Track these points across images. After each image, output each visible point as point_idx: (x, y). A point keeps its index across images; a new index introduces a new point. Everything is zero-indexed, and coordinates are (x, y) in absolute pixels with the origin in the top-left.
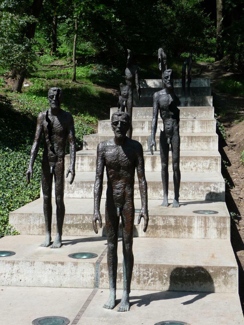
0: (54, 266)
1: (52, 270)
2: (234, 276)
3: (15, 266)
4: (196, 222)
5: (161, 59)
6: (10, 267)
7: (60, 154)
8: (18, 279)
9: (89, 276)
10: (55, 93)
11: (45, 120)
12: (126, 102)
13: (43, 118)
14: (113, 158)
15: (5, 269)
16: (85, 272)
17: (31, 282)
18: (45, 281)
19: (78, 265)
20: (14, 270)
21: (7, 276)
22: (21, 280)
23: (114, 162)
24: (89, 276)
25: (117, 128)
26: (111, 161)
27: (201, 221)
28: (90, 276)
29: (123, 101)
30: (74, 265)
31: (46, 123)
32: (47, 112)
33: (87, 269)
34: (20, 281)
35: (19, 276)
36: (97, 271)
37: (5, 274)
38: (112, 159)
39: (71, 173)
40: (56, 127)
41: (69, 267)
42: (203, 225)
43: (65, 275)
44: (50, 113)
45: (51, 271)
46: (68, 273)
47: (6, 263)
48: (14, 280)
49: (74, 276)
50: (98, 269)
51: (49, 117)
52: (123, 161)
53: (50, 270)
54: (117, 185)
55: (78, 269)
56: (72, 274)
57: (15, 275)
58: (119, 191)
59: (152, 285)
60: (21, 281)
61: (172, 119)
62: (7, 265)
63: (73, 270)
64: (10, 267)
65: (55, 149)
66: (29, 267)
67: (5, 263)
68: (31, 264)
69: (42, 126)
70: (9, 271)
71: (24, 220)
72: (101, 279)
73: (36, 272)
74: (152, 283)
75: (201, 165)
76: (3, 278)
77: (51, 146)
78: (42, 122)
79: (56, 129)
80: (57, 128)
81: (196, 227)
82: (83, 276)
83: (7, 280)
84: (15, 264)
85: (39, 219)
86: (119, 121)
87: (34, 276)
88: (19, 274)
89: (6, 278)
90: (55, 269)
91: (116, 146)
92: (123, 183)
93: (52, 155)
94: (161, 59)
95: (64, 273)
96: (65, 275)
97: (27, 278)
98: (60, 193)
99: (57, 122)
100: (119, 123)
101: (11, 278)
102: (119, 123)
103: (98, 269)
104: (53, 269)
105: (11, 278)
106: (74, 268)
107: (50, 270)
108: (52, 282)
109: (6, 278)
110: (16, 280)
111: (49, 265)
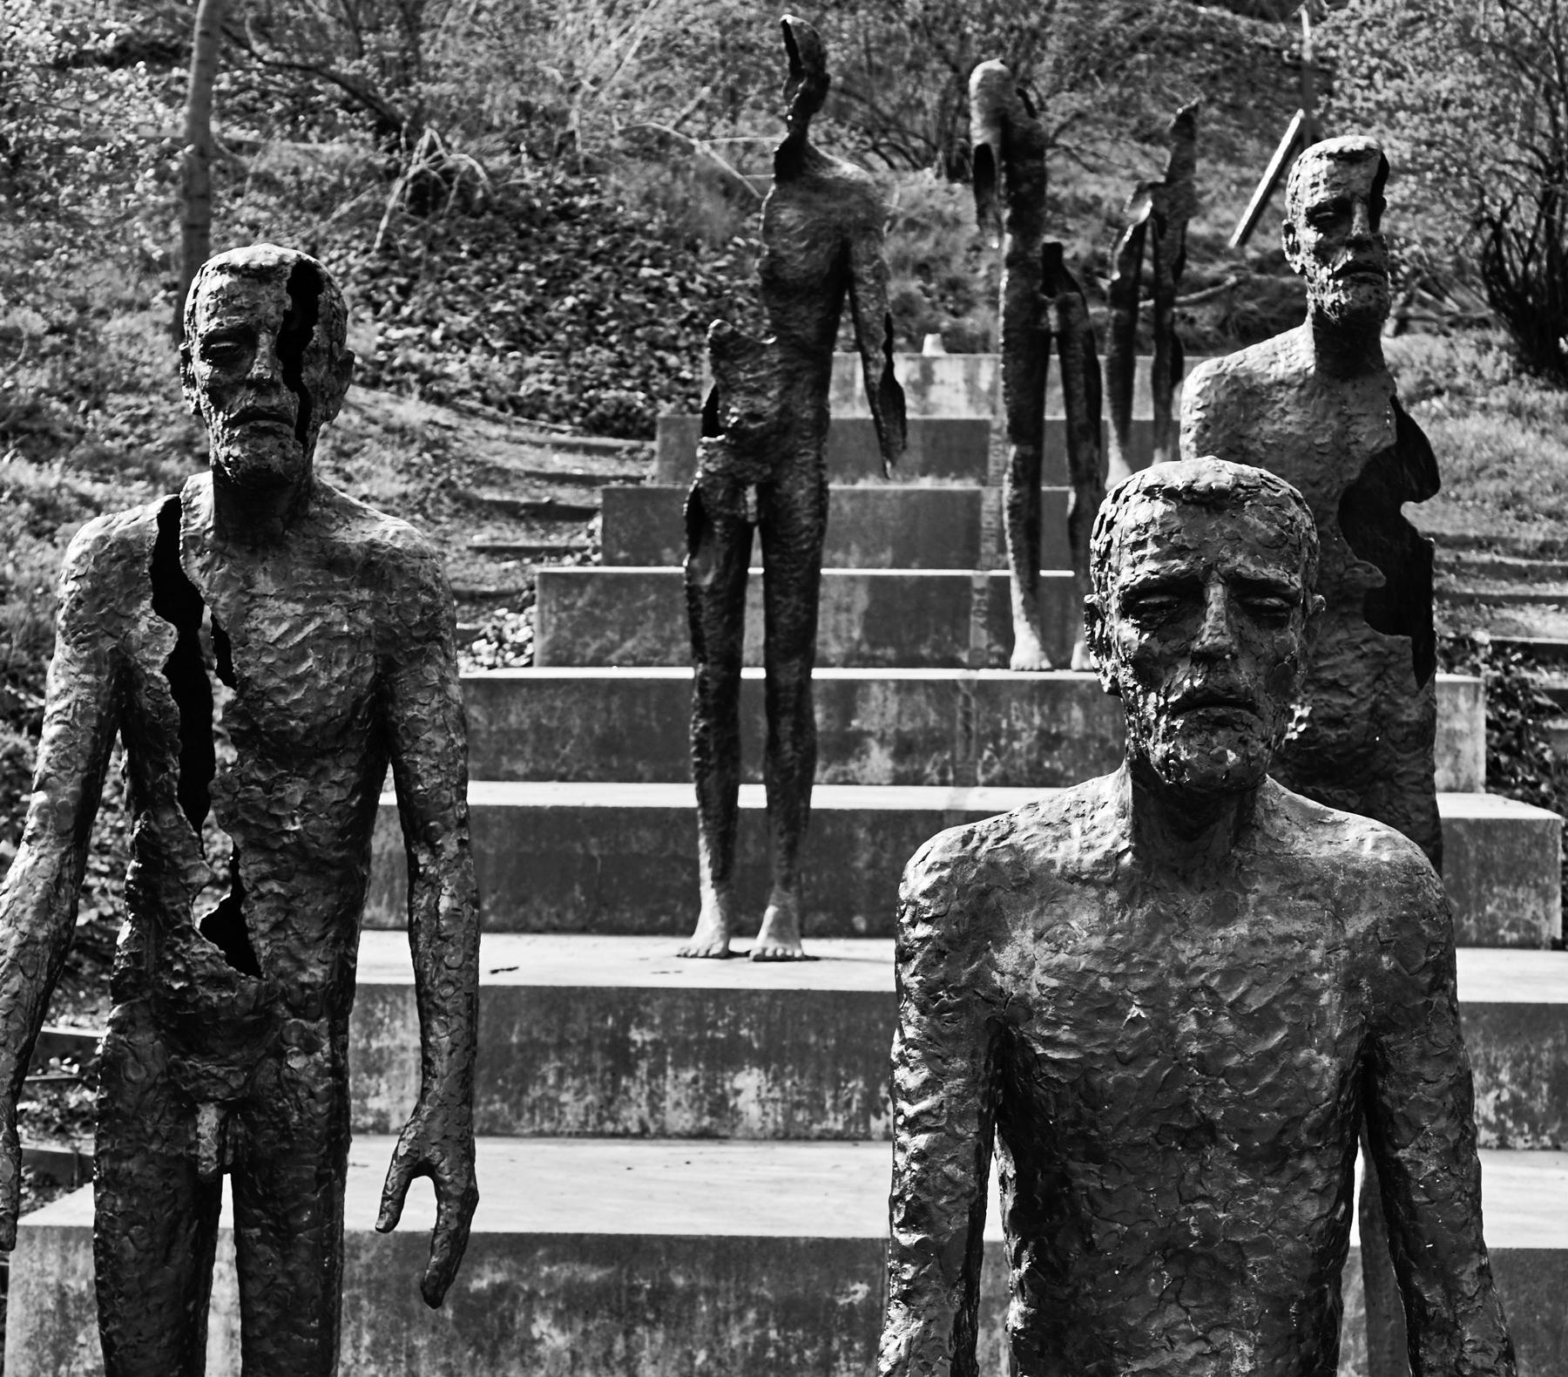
5: (995, 149)
7: (302, 966)
11: (146, 604)
13: (129, 578)
14: (1102, 1024)
23: (1120, 1083)
25: (1183, 668)
26: (1084, 1068)
31: (156, 632)
32: (171, 515)
38: (1090, 1046)
39: (438, 1183)
40: (270, 670)
52: (1234, 1061)
61: (1368, 632)
65: (258, 917)
79: (265, 694)
80: (273, 682)
86: (1209, 568)
94: (995, 149)
99: (277, 621)
100: (1216, 594)
102: (1216, 594)
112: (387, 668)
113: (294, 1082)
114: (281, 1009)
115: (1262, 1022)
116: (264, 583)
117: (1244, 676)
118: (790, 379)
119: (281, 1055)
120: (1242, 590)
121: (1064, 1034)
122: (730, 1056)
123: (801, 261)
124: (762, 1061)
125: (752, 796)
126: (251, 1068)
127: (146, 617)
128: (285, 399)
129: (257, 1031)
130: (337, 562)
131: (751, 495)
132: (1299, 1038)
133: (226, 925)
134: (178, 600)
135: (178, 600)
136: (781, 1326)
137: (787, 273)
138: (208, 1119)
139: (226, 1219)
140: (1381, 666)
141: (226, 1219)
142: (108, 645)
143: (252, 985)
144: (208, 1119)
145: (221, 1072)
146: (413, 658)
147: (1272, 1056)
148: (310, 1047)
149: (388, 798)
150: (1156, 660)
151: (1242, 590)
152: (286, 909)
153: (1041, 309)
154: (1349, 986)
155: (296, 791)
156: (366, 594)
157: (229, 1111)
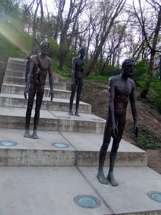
0: (50, 153)
1: (49, 156)
2: (145, 157)
3: (24, 153)
4: (98, 125)
6: (20, 153)
8: (25, 161)
9: (71, 159)
10: (48, 45)
14: (121, 88)
15: (16, 155)
16: (69, 157)
17: (35, 163)
18: (44, 163)
19: (65, 152)
20: (23, 155)
21: (18, 159)
22: (28, 162)
24: (71, 159)
27: (100, 125)
28: (72, 159)
30: (63, 152)
33: (70, 155)
34: (27, 163)
35: (26, 159)
36: (76, 156)
37: (17, 158)
41: (59, 153)
42: (101, 127)
43: (56, 158)
46: (59, 157)
47: (17, 151)
48: (23, 162)
49: (62, 159)
50: (77, 154)
51: (39, 59)
52: (127, 91)
53: (47, 155)
54: (119, 106)
55: (65, 155)
56: (61, 158)
57: (23, 159)
58: (120, 110)
59: (107, 163)
60: (28, 163)
62: (18, 152)
63: (62, 156)
64: (20, 153)
65: (40, 79)
66: (33, 153)
67: (17, 151)
68: (34, 152)
70: (19, 157)
71: (4, 119)
72: (78, 161)
73: (37, 157)
74: (107, 162)
75: (68, 96)
76: (15, 161)
77: (38, 76)
81: (97, 127)
82: (68, 159)
83: (18, 162)
84: (24, 151)
85: (14, 119)
87: (37, 159)
88: (27, 158)
89: (17, 161)
90: (50, 155)
92: (123, 105)
95: (56, 157)
96: (56, 158)
97: (32, 161)
101: (21, 161)
103: (77, 154)
104: (49, 155)
105: (21, 161)
106: (62, 154)
107: (47, 155)
108: (48, 163)
109: (17, 161)
110: (24, 162)
111: (47, 152)
114: (41, 84)
116: (43, 60)
119: (41, 87)
121: (119, 88)
126: (39, 88)
129: (40, 85)
142: (34, 63)
143: (40, 83)
145: (37, 88)
146: (51, 66)
147: (129, 91)
150: (128, 69)
155: (44, 72)
156: (49, 62)
157: (37, 90)
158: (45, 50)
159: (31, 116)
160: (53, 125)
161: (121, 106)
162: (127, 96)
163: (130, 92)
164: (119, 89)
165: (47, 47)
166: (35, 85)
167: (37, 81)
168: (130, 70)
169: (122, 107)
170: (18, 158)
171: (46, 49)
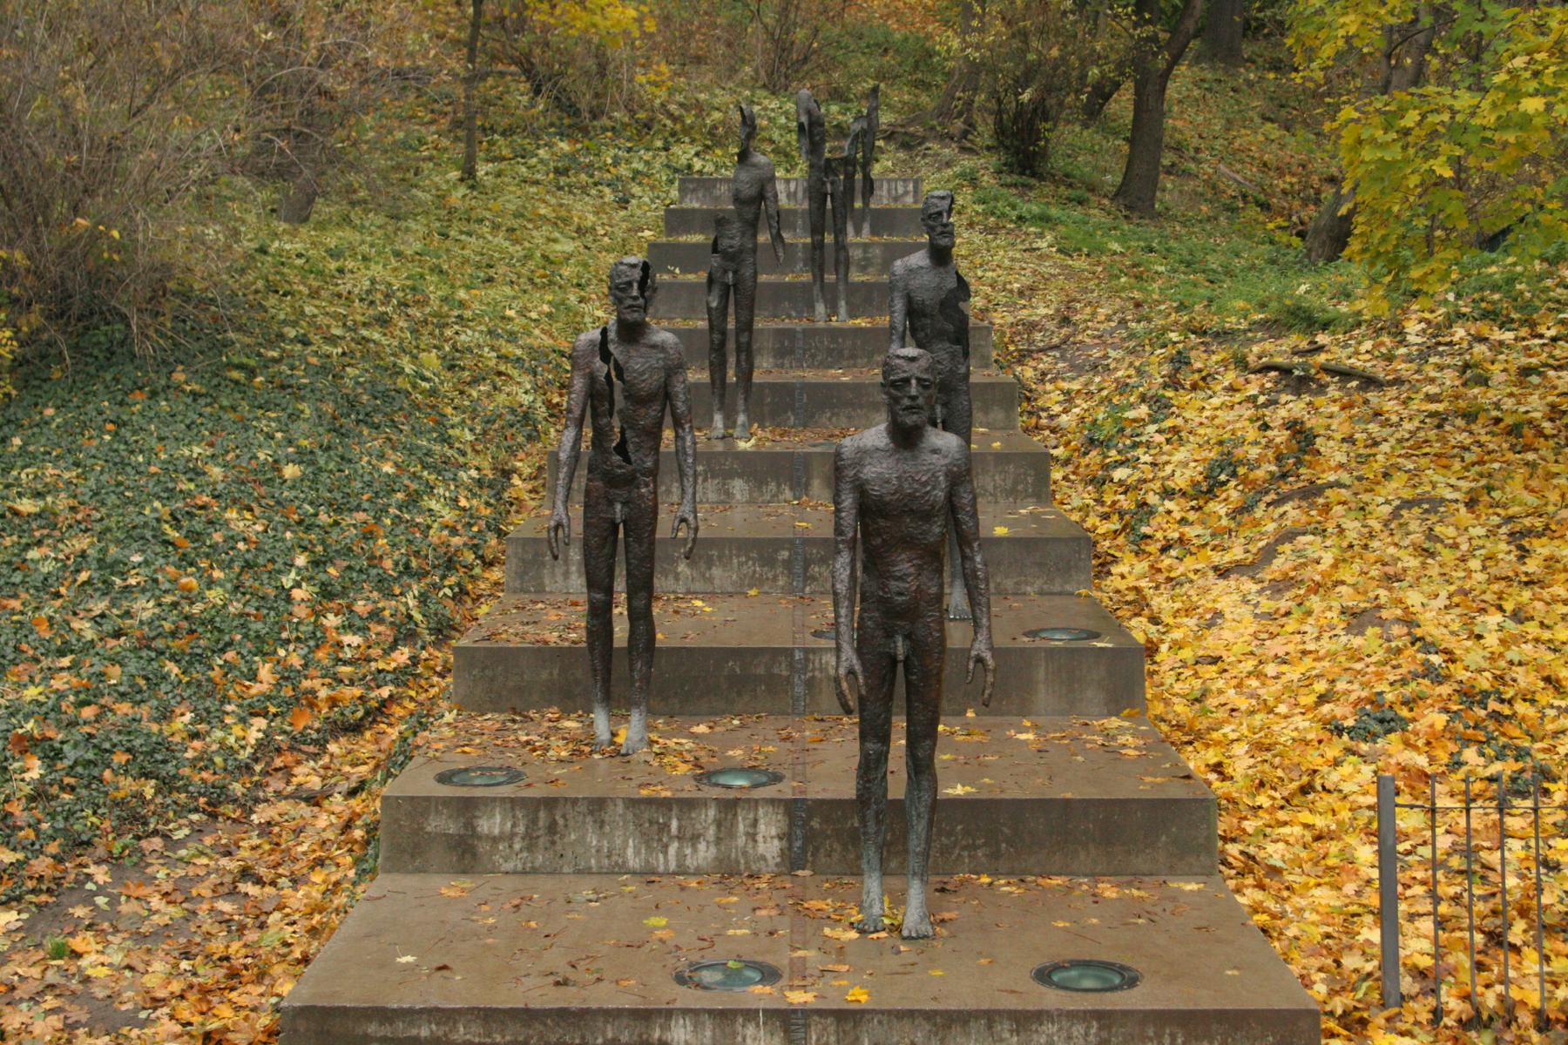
10: (637, 274)
12: (735, 272)
13: (593, 351)
29: (726, 272)
32: (604, 332)
37: (513, 835)
44: (612, 335)
45: (655, 827)
51: (611, 347)
58: (902, 585)
65: (631, 447)
69: (592, 379)
74: (966, 853)
78: (588, 365)
91: (896, 451)
93: (620, 467)
98: (642, 589)
100: (914, 382)
102: (914, 382)
112: (668, 377)
113: (642, 496)
115: (925, 484)
117: (920, 401)
118: (743, 234)
120: (919, 380)
122: (729, 475)
123: (748, 191)
124: (740, 476)
125: (731, 377)
127: (598, 363)
128: (641, 301)
129: (630, 481)
130: (654, 346)
131: (730, 275)
132: (934, 488)
133: (621, 448)
134: (606, 356)
135: (606, 356)
136: (762, 566)
137: (742, 196)
138: (618, 507)
139: (621, 535)
140: (953, 356)
141: (621, 535)
143: (630, 468)
144: (618, 507)
145: (623, 493)
148: (647, 485)
149: (668, 409)
151: (919, 380)
152: (639, 447)
153: (824, 183)
154: (946, 475)
155: (643, 411)
157: (624, 504)
158: (629, 302)
159: (616, 645)
160: (775, 686)
161: (904, 564)
162: (927, 516)
163: (940, 494)
164: (876, 490)
165: (635, 285)
166: (612, 481)
167: (617, 458)
168: (906, 402)
169: (912, 570)
170: (517, 839)
171: (635, 298)
